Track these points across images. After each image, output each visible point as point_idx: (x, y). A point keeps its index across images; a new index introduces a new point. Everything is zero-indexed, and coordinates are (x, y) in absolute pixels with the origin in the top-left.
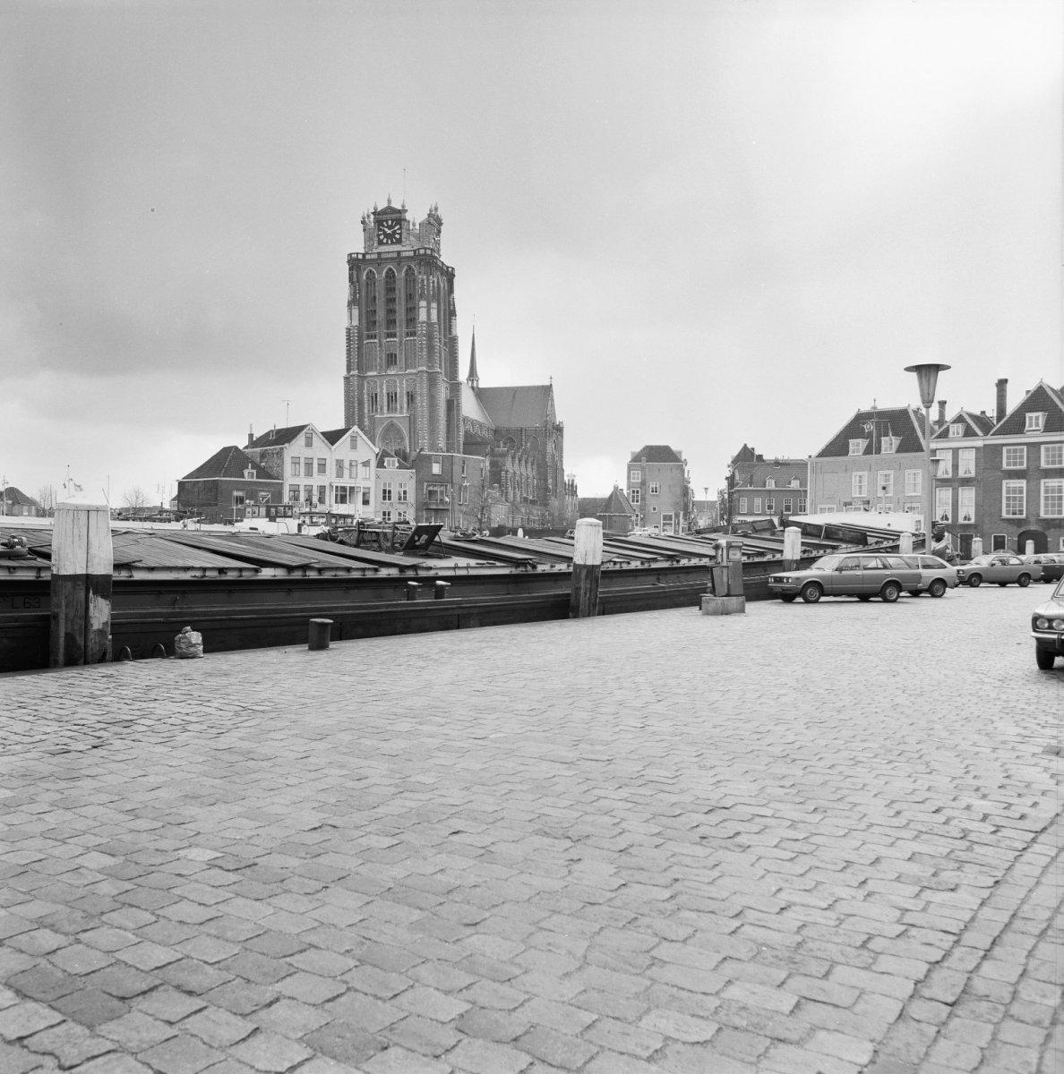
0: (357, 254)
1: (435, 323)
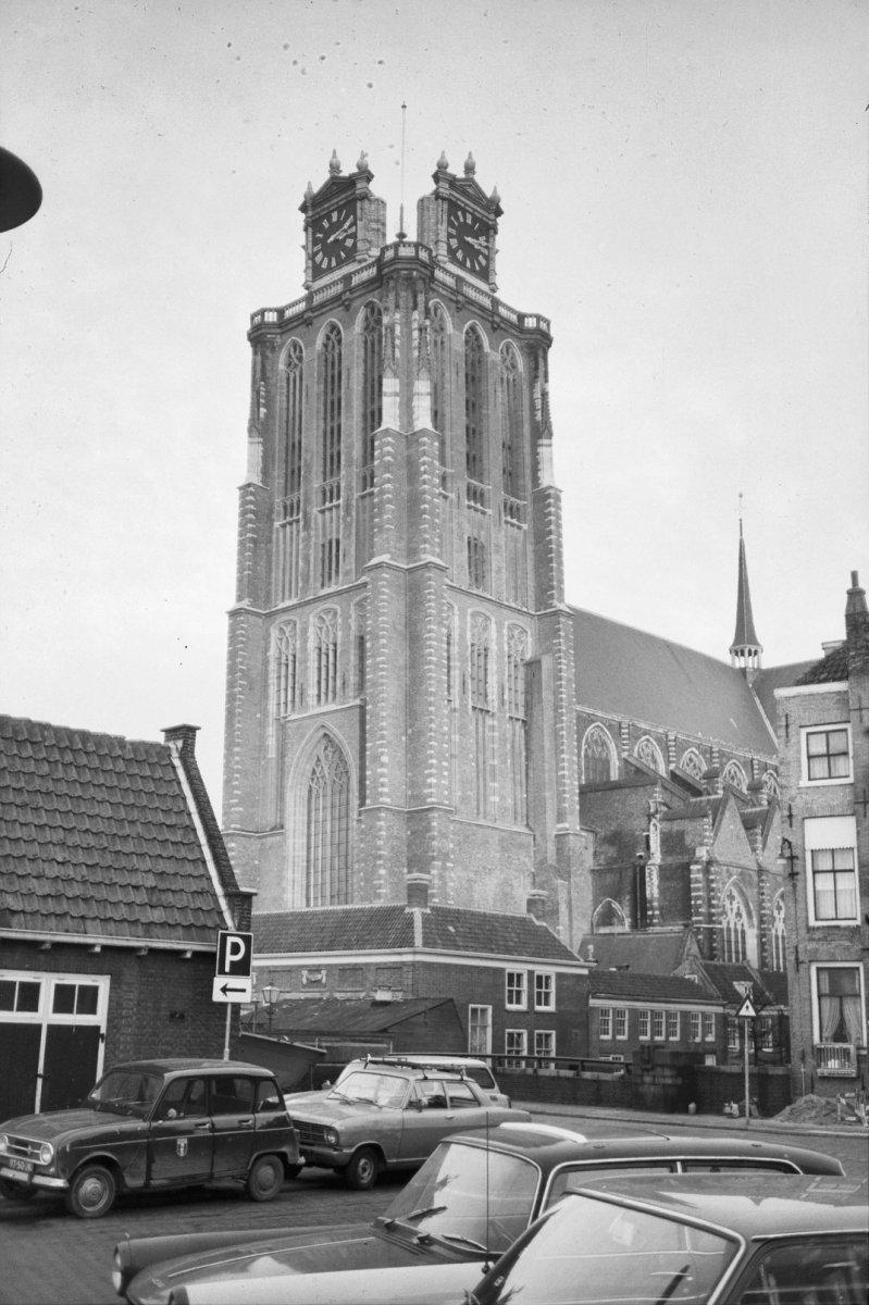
0: (262, 312)
1: (424, 432)
